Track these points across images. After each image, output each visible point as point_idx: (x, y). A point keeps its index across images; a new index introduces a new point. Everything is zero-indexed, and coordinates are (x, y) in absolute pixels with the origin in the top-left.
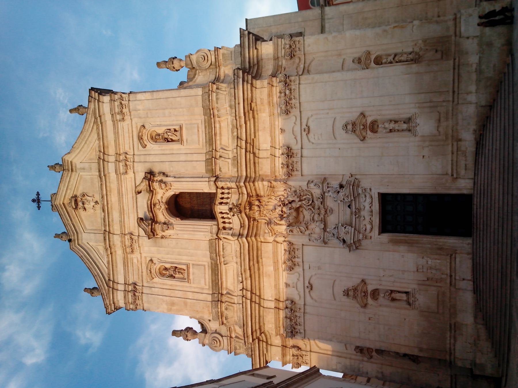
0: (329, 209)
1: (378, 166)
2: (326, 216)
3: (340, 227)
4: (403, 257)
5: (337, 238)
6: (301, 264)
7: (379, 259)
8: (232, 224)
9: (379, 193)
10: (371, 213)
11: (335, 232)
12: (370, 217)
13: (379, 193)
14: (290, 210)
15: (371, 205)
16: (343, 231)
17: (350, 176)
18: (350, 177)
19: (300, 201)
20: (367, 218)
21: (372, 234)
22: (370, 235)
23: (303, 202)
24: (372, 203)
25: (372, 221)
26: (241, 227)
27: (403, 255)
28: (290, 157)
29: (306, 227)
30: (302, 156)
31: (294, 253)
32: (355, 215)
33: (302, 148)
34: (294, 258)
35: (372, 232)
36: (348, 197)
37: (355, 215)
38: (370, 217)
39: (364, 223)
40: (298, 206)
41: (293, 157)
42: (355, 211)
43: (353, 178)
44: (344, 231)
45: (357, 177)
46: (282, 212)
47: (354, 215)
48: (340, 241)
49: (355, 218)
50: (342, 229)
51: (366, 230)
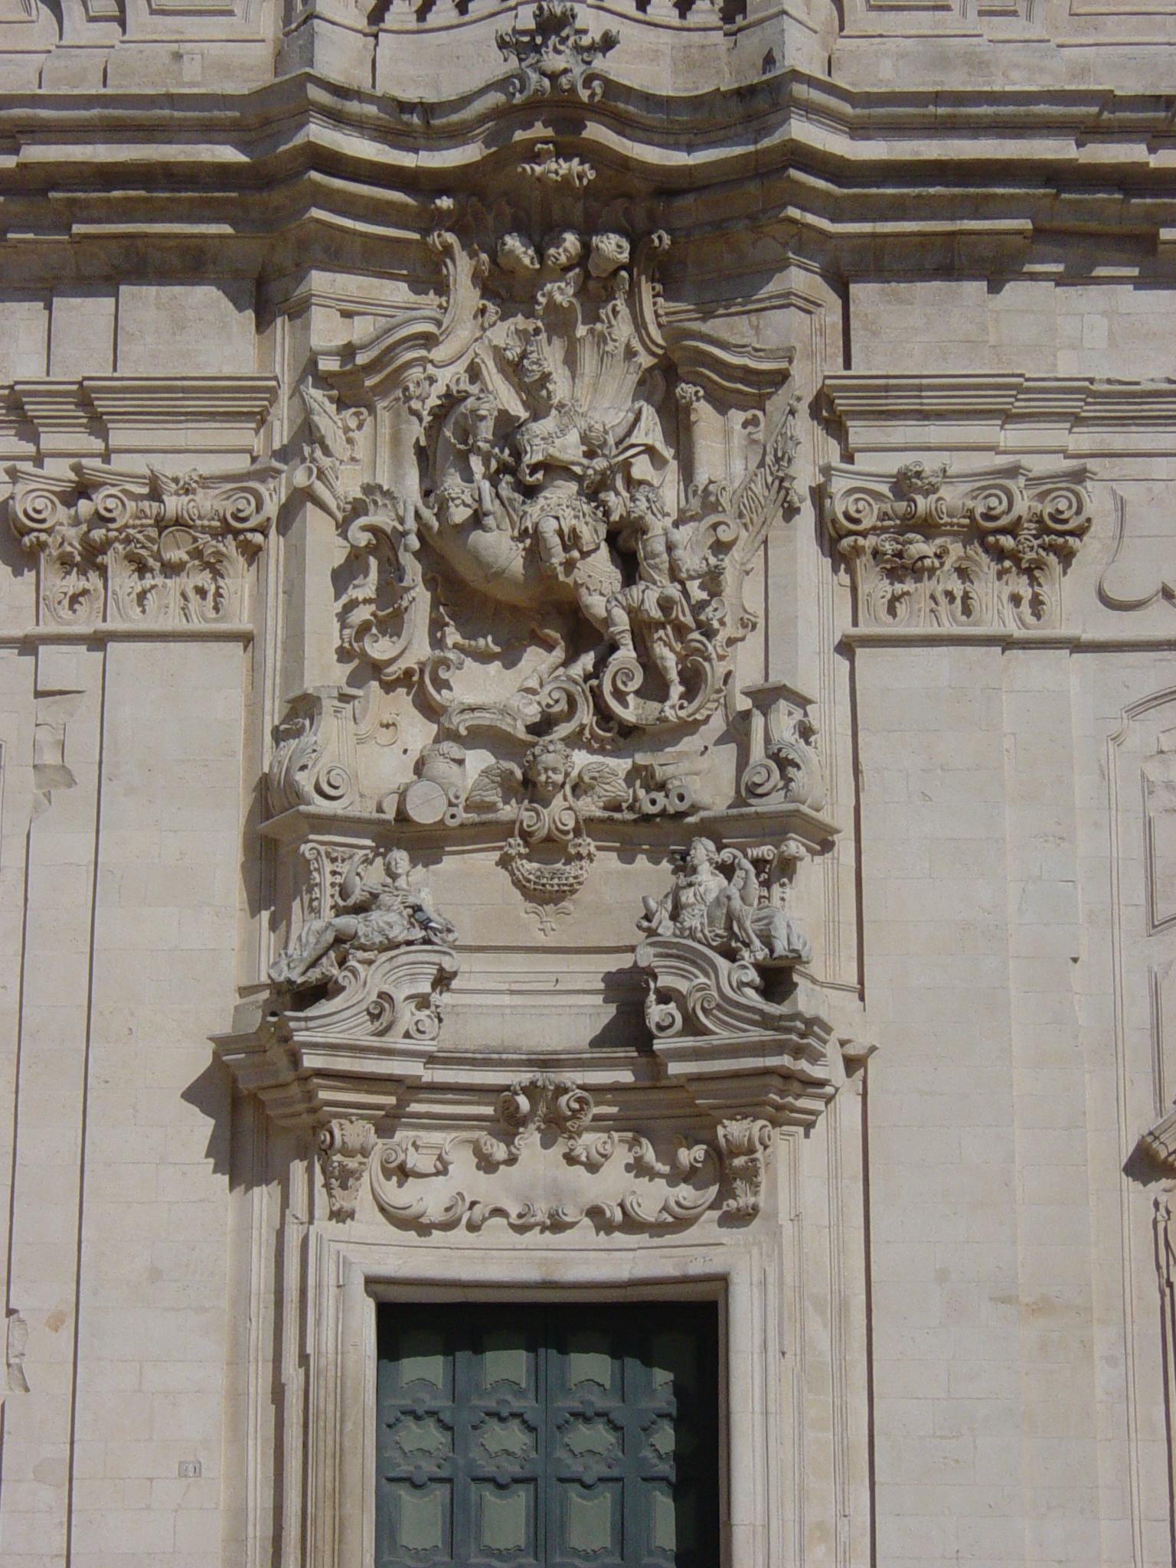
0: (572, 869)
1: (943, 1276)
2: (516, 845)
3: (435, 958)
4: (183, 1474)
5: (339, 940)
6: (84, 622)
7: (155, 1274)
8: (412, 23)
9: (723, 1280)
10: (541, 1216)
11: (389, 921)
12: (514, 1211)
13: (723, 1280)
14: (560, 533)
15: (619, 1216)
16: (397, 982)
17: (851, 1050)
18: (843, 1043)
19: (642, 631)
20: (489, 1189)
21: (370, 1224)
22: (361, 1199)
23: (626, 653)
24: (631, 1224)
25: (473, 1227)
26: (405, 107)
27: (197, 1471)
28: (1007, 542)
29: (408, 673)
30: (1007, 643)
31: (172, 569)
32: (525, 1091)
33: (1077, 646)
34: (131, 558)
35: (380, 1217)
36: (692, 1026)
37: (525, 1091)
38: (514, 1211)
39: (462, 1162)
40: (596, 604)
41: (1000, 575)
42: (566, 1090)
43: (831, 1069)
44: (399, 996)
45: (848, 1105)
46: (534, 469)
47: (524, 1077)
48: (314, 964)
49: (507, 1088)
50: (413, 977)
51: (403, 1173)
